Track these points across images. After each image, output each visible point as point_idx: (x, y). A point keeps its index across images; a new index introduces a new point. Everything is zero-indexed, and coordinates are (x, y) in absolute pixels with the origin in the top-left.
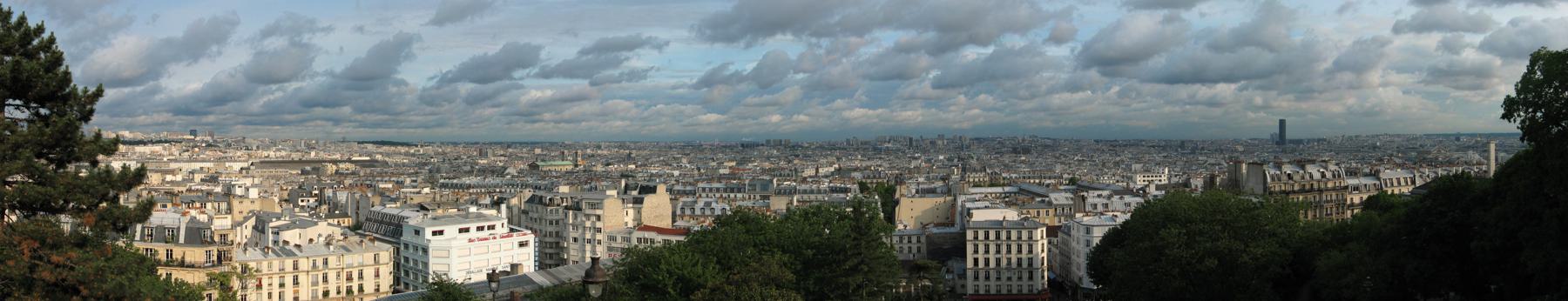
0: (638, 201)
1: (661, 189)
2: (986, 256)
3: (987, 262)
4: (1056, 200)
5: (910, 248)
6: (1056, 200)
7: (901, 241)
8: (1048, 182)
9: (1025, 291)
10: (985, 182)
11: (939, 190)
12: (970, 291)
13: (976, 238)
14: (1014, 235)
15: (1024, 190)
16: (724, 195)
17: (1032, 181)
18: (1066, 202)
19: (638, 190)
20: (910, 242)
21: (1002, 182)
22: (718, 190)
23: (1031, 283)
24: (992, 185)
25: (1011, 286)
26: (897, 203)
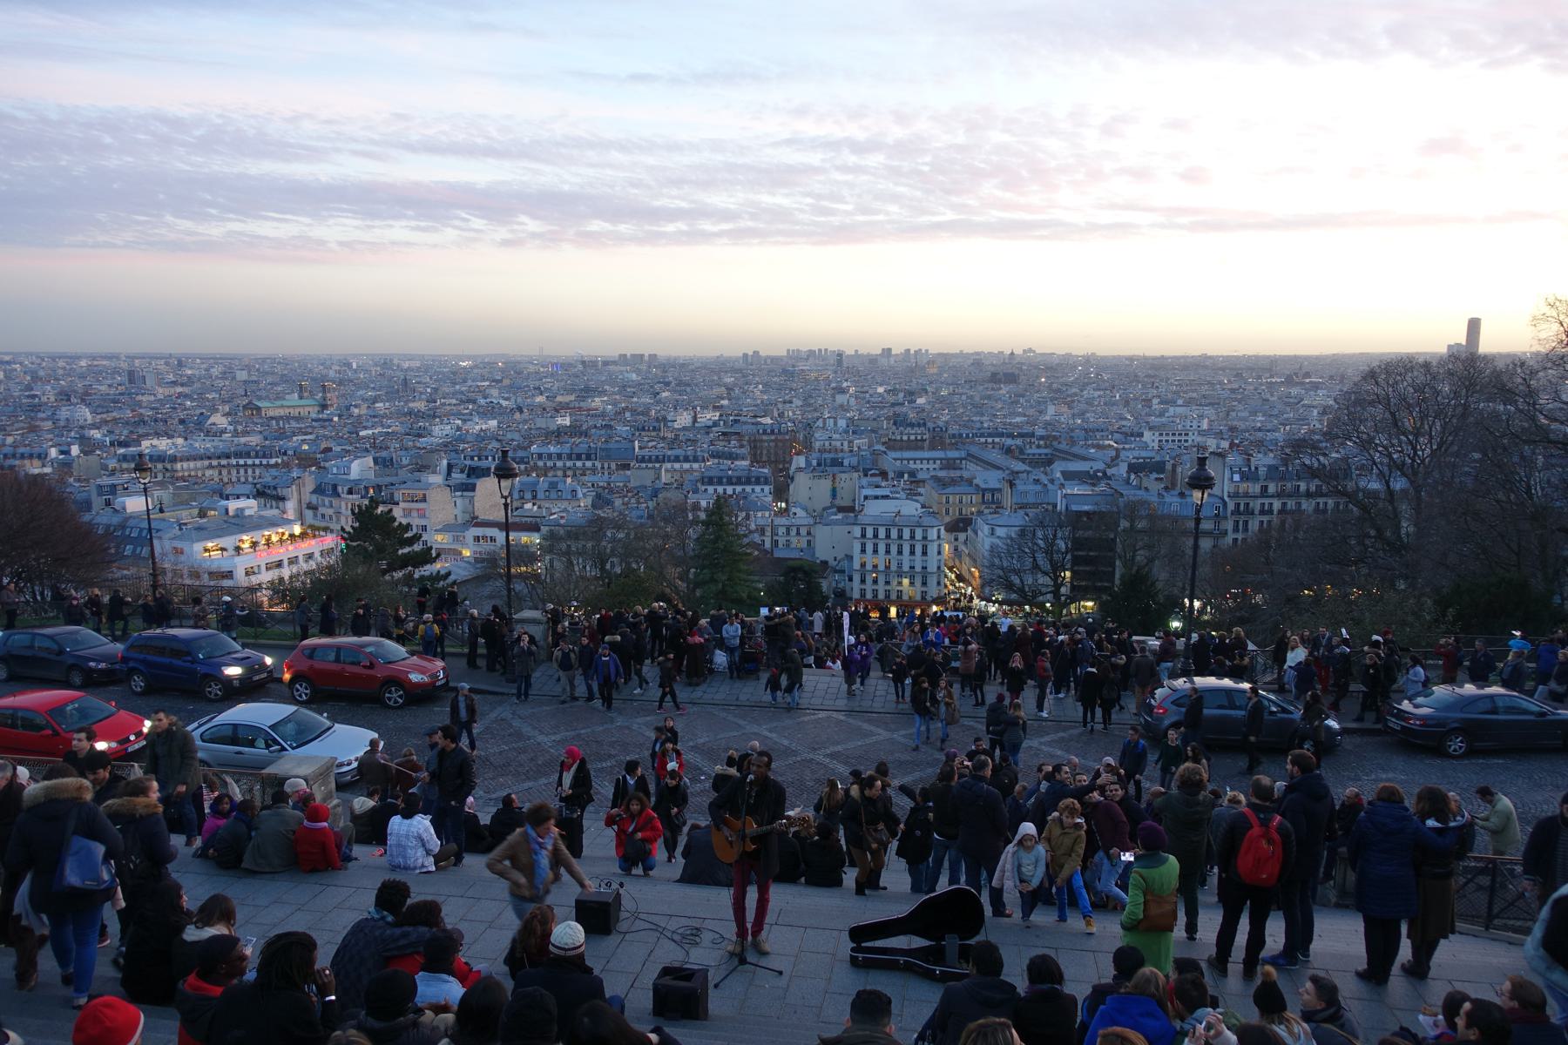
0: (472, 488)
7: (788, 533)
10: (923, 440)
11: (846, 463)
13: (863, 536)
14: (906, 534)
15: (973, 456)
16: (569, 464)
17: (990, 440)
18: (998, 486)
20: (798, 533)
21: (948, 441)
22: (559, 456)
23: (924, 589)
24: (933, 448)
26: (792, 479)
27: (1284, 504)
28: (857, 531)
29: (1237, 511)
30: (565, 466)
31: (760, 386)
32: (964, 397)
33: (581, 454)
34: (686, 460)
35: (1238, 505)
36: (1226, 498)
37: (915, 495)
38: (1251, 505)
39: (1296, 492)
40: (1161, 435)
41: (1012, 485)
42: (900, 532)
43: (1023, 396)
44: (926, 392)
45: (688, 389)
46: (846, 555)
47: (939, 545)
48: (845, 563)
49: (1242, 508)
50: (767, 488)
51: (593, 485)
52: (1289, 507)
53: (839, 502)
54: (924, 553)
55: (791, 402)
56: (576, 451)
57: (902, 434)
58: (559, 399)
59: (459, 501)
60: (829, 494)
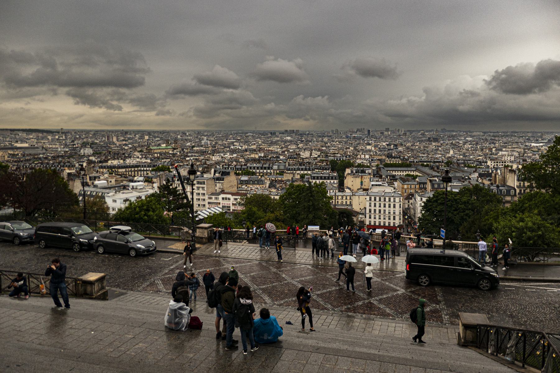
1: (232, 174)
2: (375, 208)
3: (375, 210)
5: (346, 202)
7: (342, 199)
11: (367, 171)
12: (367, 223)
13: (370, 200)
15: (418, 170)
16: (261, 171)
17: (425, 164)
18: (425, 181)
20: (346, 199)
22: (258, 168)
23: (394, 221)
26: (345, 178)
28: (368, 198)
30: (260, 171)
32: (417, 147)
35: (521, 191)
36: (516, 188)
37: (392, 184)
40: (495, 163)
45: (310, 143)
47: (400, 204)
48: (364, 211)
49: (522, 192)
50: (336, 181)
55: (349, 148)
56: (264, 166)
57: (390, 161)
58: (261, 147)
59: (218, 185)
60: (359, 184)
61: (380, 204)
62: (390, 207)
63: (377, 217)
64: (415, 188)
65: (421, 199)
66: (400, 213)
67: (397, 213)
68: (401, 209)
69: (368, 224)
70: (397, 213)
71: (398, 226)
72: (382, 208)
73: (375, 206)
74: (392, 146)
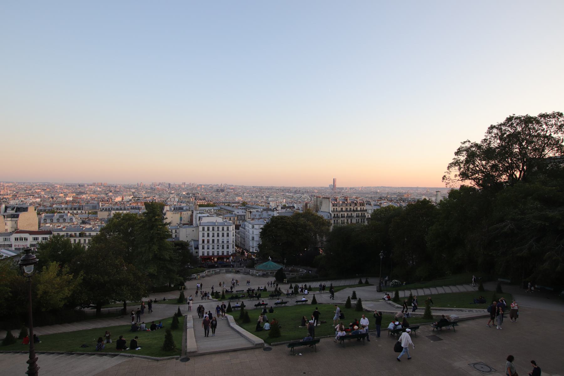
0: (17, 216)
1: (31, 209)
3: (208, 242)
4: (238, 213)
6: (238, 213)
8: (233, 205)
9: (225, 254)
11: (184, 208)
12: (201, 254)
13: (203, 229)
15: (222, 209)
16: (71, 211)
17: (226, 204)
18: (242, 214)
19: (15, 210)
25: (219, 252)
27: (348, 214)
28: (201, 228)
29: (334, 217)
31: (144, 192)
32: (210, 195)
33: (76, 208)
34: (121, 209)
35: (335, 214)
36: (331, 212)
37: (220, 215)
38: (338, 215)
39: (350, 211)
41: (251, 212)
42: (218, 228)
43: (227, 195)
44: (198, 194)
45: (119, 193)
46: (192, 240)
48: (192, 243)
49: (336, 216)
51: (81, 218)
52: (349, 215)
53: (182, 222)
54: (228, 236)
60: (179, 219)
61: (213, 234)
62: (223, 236)
63: (211, 247)
64: (234, 219)
65: (253, 227)
66: (233, 241)
67: (231, 242)
68: (234, 237)
69: (201, 255)
70: (231, 242)
71: (232, 255)
72: (216, 238)
73: (208, 236)
74: (191, 195)
